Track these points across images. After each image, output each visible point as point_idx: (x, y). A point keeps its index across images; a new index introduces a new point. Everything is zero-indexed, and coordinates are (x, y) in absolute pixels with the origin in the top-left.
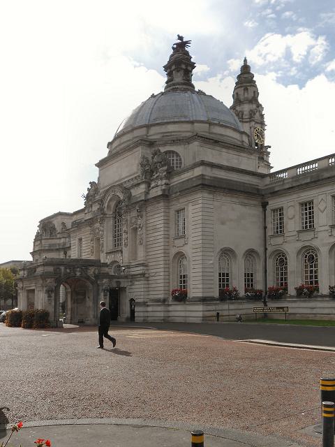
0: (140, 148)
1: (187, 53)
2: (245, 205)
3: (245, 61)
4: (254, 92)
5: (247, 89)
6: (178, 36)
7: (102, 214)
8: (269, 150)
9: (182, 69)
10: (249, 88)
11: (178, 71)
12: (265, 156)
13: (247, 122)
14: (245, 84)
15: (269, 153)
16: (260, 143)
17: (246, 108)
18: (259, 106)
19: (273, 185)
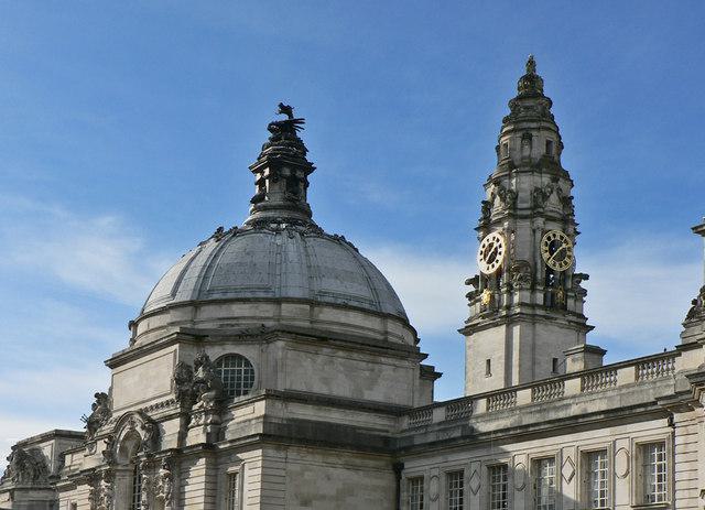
1: (299, 144)
2: (356, 468)
3: (531, 63)
4: (549, 143)
6: (281, 105)
7: (109, 463)
8: (583, 284)
9: (283, 177)
10: (534, 133)
12: (570, 302)
13: (526, 217)
14: (525, 125)
15: (584, 292)
16: (557, 268)
17: (523, 184)
18: (559, 174)
19: (413, 433)
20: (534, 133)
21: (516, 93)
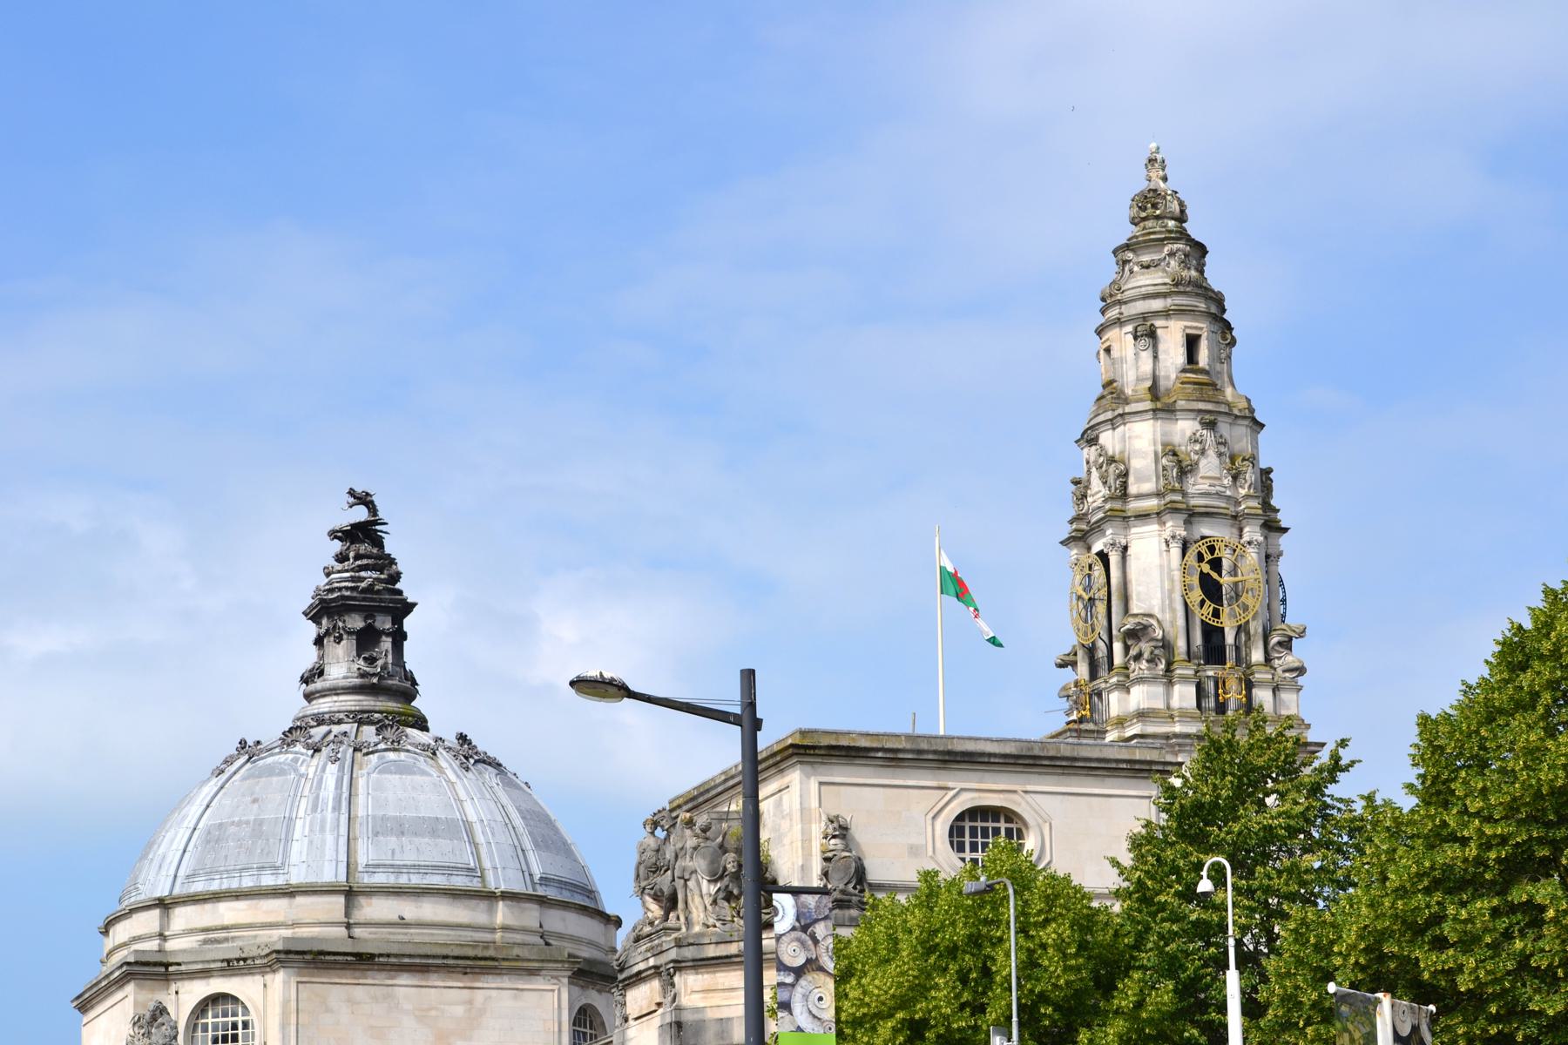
0: (130, 988)
5: (1152, 334)
10: (1158, 323)
11: (339, 640)
20: (1158, 323)
21: (1126, 231)
